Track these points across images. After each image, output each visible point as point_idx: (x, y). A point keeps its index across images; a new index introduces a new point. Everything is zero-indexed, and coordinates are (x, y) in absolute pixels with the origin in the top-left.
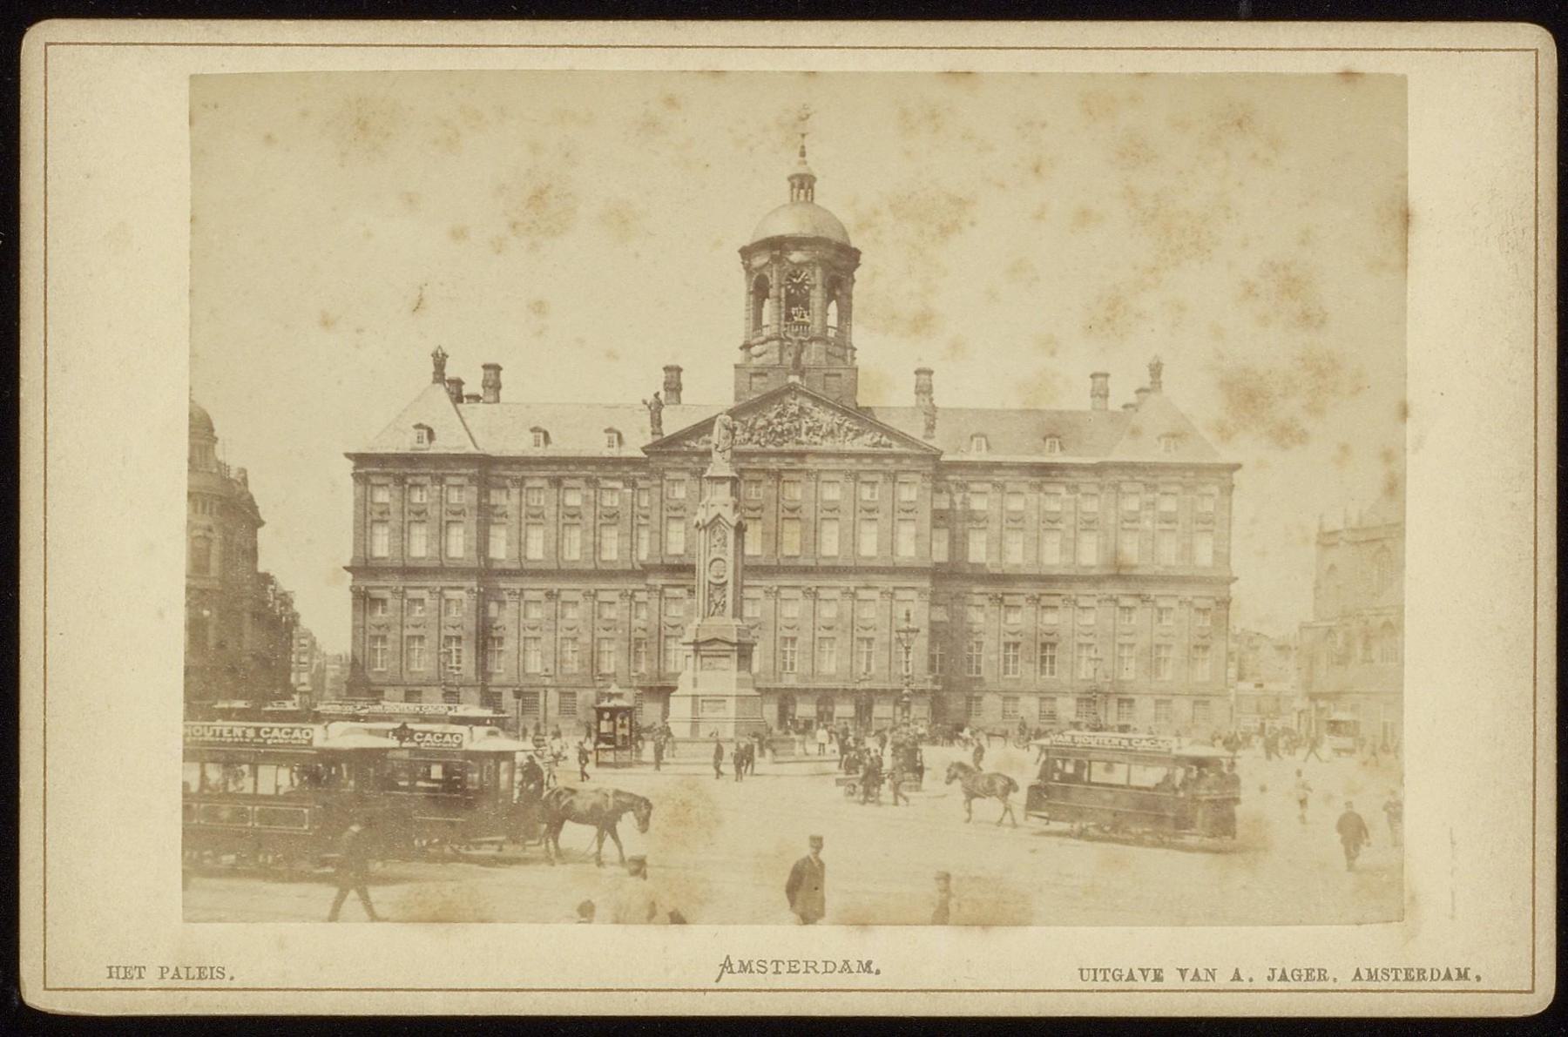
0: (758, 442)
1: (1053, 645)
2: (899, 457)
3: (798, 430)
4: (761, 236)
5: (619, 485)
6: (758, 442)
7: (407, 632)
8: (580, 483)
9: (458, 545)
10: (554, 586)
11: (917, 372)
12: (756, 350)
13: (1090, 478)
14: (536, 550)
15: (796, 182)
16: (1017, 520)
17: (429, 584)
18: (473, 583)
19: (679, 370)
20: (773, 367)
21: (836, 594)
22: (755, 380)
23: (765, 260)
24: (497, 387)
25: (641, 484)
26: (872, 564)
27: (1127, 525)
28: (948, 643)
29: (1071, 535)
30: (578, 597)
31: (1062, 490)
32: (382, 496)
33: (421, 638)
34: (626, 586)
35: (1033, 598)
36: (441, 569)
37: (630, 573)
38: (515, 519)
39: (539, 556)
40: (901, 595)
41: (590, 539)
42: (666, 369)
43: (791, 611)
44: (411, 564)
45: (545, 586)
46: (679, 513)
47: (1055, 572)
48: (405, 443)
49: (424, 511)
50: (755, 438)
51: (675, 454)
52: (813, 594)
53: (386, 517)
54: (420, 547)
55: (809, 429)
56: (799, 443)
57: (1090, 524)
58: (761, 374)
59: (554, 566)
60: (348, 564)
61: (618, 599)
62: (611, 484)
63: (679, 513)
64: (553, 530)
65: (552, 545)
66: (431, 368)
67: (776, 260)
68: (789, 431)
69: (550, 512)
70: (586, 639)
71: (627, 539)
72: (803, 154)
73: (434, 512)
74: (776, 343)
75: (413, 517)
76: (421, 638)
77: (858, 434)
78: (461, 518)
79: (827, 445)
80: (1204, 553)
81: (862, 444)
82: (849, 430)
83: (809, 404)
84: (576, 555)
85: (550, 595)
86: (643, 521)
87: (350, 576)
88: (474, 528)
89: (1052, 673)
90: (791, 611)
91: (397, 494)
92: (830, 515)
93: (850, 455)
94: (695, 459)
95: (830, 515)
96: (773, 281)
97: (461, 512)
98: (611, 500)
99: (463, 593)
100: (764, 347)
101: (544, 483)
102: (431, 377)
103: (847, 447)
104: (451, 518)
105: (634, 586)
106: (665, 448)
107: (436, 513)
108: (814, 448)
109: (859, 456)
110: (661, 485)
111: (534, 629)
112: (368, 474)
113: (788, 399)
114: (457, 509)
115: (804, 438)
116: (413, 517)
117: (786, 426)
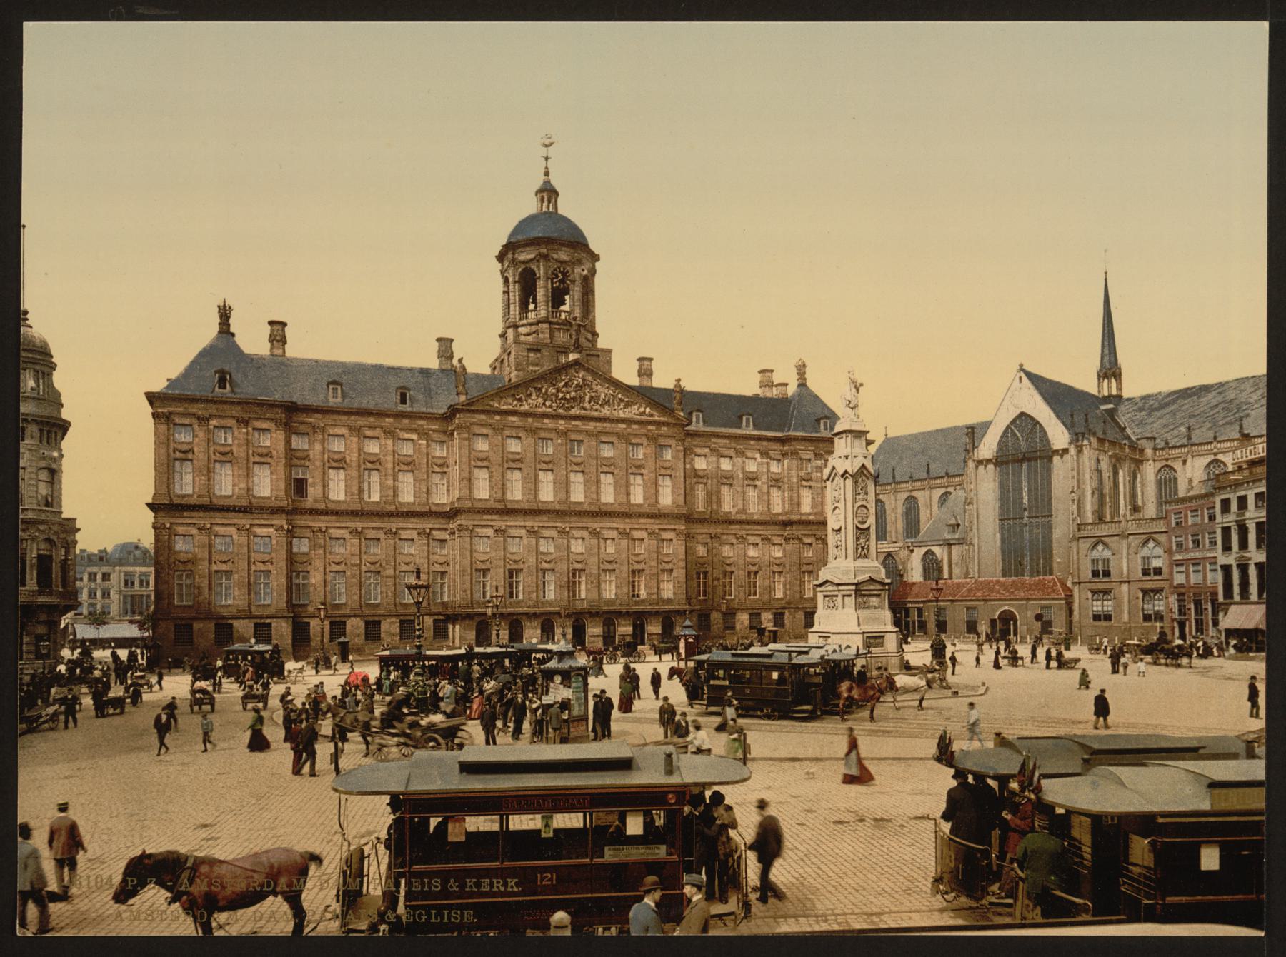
0: (551, 407)
1: (756, 573)
2: (658, 424)
3: (582, 399)
4: (520, 237)
5: (415, 437)
6: (551, 407)
7: (215, 568)
8: (377, 432)
9: (266, 485)
10: (359, 524)
11: (639, 360)
12: (521, 330)
13: (777, 446)
14: (338, 490)
15: (545, 195)
16: (727, 479)
17: (274, 522)
18: (281, 521)
19: (452, 340)
20: (546, 345)
21: (489, 532)
22: (531, 355)
23: (532, 256)
24: (283, 341)
25: (435, 436)
26: (642, 510)
27: (804, 483)
28: (698, 572)
29: (765, 489)
30: (381, 535)
31: (758, 456)
32: (183, 437)
33: (228, 573)
34: (424, 526)
35: (653, 533)
36: (248, 508)
37: (355, 514)
38: (318, 463)
39: (342, 497)
40: (666, 535)
41: (390, 482)
42: (439, 340)
43: (577, 547)
44: (177, 501)
45: (349, 524)
46: (485, 463)
47: (755, 518)
48: (207, 384)
49: (231, 452)
50: (548, 403)
51: (477, 412)
52: (595, 534)
53: (190, 456)
54: (226, 484)
55: (592, 397)
56: (585, 409)
57: (776, 482)
58: (538, 350)
59: (322, 506)
60: (150, 501)
61: (415, 537)
62: (407, 436)
63: (485, 463)
64: (355, 474)
65: (355, 489)
66: (218, 320)
67: (546, 257)
68: (574, 399)
69: (352, 457)
70: (390, 572)
71: (424, 483)
72: (547, 174)
73: (239, 452)
74: (546, 326)
75: (219, 457)
76: (228, 573)
77: (628, 405)
78: (269, 460)
79: (606, 411)
80: (806, 507)
81: (633, 412)
82: (621, 400)
83: (590, 378)
84: (376, 497)
85: (354, 532)
86: (437, 469)
87: (66, 514)
88: (281, 469)
89: (755, 594)
90: (577, 547)
91: (201, 434)
92: (606, 469)
93: (623, 421)
94: (498, 417)
95: (606, 469)
96: (541, 271)
97: (269, 454)
98: (407, 450)
99: (271, 530)
100: (534, 328)
101: (344, 431)
102: (216, 329)
103: (622, 415)
104: (257, 459)
105: (430, 526)
106: (469, 408)
107: (243, 454)
108: (596, 414)
109: (629, 421)
110: (469, 439)
111: (338, 564)
112: (170, 413)
113: (572, 371)
114: (265, 451)
115: (586, 405)
116: (219, 457)
117: (573, 394)
